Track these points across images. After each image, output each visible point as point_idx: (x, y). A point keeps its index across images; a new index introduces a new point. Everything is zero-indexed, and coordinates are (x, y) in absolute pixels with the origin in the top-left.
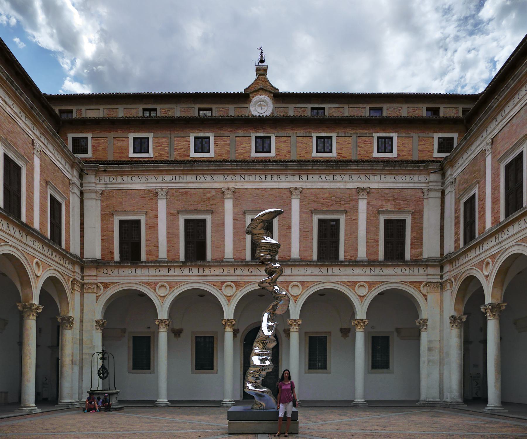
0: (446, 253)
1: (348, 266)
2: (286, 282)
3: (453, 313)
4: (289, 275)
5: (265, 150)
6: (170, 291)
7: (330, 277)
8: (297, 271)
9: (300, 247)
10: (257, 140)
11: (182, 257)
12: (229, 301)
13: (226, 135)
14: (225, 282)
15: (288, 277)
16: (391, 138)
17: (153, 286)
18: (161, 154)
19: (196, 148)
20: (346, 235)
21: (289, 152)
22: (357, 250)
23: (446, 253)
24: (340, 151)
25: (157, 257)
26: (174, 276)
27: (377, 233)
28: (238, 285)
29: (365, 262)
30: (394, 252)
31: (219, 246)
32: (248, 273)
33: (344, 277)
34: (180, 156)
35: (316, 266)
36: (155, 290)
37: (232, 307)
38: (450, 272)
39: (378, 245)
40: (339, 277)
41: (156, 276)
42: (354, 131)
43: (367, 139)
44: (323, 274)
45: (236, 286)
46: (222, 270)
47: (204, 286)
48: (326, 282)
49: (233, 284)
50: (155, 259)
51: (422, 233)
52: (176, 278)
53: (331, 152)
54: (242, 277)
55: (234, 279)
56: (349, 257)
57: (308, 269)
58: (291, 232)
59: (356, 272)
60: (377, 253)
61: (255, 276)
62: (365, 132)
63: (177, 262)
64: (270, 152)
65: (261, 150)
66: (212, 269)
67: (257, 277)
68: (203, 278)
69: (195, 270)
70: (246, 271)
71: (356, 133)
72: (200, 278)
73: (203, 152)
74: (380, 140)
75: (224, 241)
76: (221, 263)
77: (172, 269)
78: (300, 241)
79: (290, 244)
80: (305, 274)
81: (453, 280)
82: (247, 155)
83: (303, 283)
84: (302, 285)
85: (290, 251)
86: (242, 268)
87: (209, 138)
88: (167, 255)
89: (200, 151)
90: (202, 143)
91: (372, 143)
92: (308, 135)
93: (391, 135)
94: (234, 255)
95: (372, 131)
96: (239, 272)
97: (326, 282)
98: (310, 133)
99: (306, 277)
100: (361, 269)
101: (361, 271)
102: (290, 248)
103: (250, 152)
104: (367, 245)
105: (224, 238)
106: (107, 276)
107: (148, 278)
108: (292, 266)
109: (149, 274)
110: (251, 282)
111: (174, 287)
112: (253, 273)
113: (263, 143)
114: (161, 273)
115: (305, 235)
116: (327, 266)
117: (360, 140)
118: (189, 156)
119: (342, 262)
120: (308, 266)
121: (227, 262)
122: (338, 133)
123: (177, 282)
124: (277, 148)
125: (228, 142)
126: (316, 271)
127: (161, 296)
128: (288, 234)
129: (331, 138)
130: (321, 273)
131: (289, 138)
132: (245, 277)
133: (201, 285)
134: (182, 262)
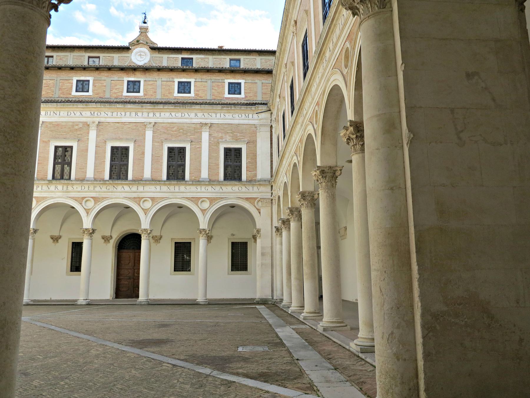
1: (192, 184)
5: (135, 90)
7: (177, 194)
8: (147, 188)
9: (152, 169)
10: (129, 83)
11: (50, 177)
12: (88, 213)
13: (103, 79)
14: (85, 197)
15: (141, 194)
16: (240, 84)
18: (48, 93)
19: (78, 89)
20: (191, 160)
21: (155, 92)
24: (197, 93)
26: (41, 192)
27: (218, 158)
28: (96, 200)
29: (207, 182)
31: (83, 167)
33: (188, 194)
34: (63, 94)
35: (165, 185)
37: (90, 218)
39: (218, 168)
40: (184, 194)
42: (209, 78)
43: (220, 84)
44: (171, 191)
46: (83, 188)
47: (67, 200)
49: (91, 199)
51: (256, 158)
52: (43, 194)
53: (190, 93)
54: (100, 193)
55: (94, 195)
56: (193, 178)
57: (158, 187)
59: (199, 190)
60: (218, 174)
62: (218, 78)
63: (44, 180)
64: (139, 92)
65: (132, 91)
66: (75, 187)
67: (113, 194)
68: (66, 194)
69: (60, 187)
70: (104, 189)
72: (64, 194)
73: (83, 91)
74: (231, 85)
75: (86, 164)
76: (82, 180)
79: (143, 167)
80: (155, 191)
82: (119, 94)
83: (153, 199)
87: (89, 81)
89: (81, 90)
90: (82, 84)
91: (224, 87)
92: (171, 80)
93: (239, 81)
94: (94, 175)
95: (224, 78)
96: (98, 189)
98: (173, 78)
99: (156, 194)
100: (203, 188)
102: (143, 170)
103: (122, 92)
105: (87, 161)
108: (144, 185)
111: (40, 201)
112: (110, 190)
113: (134, 85)
115: (156, 159)
116: (174, 184)
117: (214, 84)
118: (71, 94)
119: (186, 181)
120: (157, 184)
121: (87, 181)
123: (44, 197)
124: (144, 90)
125: (105, 84)
126: (165, 188)
129: (190, 83)
132: (103, 194)
133: (64, 200)
134: (49, 181)
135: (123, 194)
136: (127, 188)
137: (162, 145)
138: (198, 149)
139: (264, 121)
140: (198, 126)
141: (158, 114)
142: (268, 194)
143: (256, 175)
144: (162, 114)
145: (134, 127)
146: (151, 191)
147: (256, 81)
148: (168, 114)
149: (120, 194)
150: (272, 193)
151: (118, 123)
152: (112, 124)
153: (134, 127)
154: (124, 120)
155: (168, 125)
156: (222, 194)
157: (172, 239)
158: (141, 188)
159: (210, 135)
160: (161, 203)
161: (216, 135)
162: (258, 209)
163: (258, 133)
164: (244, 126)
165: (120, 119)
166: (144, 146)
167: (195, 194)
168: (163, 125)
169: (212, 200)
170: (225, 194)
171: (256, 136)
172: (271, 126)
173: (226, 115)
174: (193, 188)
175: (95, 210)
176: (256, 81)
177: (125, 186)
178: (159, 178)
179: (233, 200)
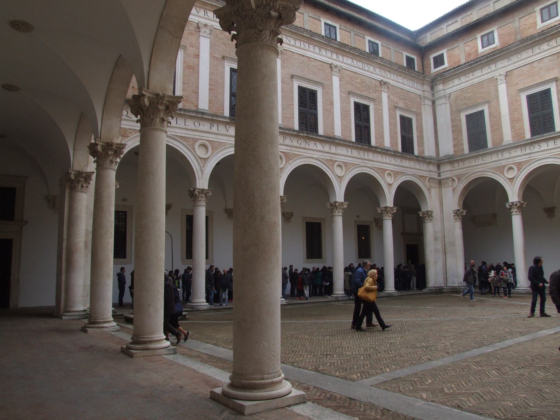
0: (442, 155)
2: (332, 160)
3: (456, 207)
4: (334, 154)
6: (212, 153)
17: (191, 143)
22: (383, 137)
23: (442, 155)
25: (197, 106)
26: (218, 134)
30: (407, 146)
32: (297, 145)
33: (376, 163)
35: (356, 148)
36: (194, 149)
38: (451, 171)
41: (196, 131)
42: (351, 28)
45: (285, 157)
48: (364, 166)
50: (193, 108)
52: (220, 137)
56: (378, 144)
58: (333, 108)
60: (397, 144)
61: (305, 149)
67: (305, 151)
71: (354, 31)
77: (215, 125)
78: (341, 120)
81: (454, 178)
84: (345, 166)
85: (333, 128)
86: (292, 138)
88: (209, 106)
91: (364, 43)
92: (317, 18)
93: (377, 42)
97: (364, 166)
99: (347, 158)
101: (387, 159)
104: (390, 136)
106: (128, 120)
107: (184, 131)
109: (187, 127)
110: (301, 155)
111: (217, 149)
112: (302, 146)
114: (202, 128)
122: (340, 26)
126: (355, 153)
127: (201, 158)
128: (331, 109)
130: (359, 156)
131: (302, 15)
132: (294, 149)
135: (316, 153)
136: (319, 146)
137: (349, 97)
138: (380, 111)
139: (428, 93)
140: (378, 84)
141: (340, 58)
142: (435, 174)
143: (423, 152)
144: (345, 58)
145: (320, 67)
146: (344, 154)
147: (390, 47)
148: (349, 61)
149: (311, 154)
150: (439, 174)
151: (303, 56)
152: (297, 56)
153: (320, 67)
154: (309, 54)
155: (352, 74)
156: (403, 168)
157: (303, 218)
158: (333, 149)
159: (388, 97)
160: (353, 171)
161: (392, 97)
162: (429, 190)
163: (422, 106)
164: (413, 95)
165: (305, 52)
166: (332, 95)
167: (381, 164)
168: (347, 72)
169: (396, 174)
170: (405, 169)
171: (421, 108)
172: (434, 103)
173: (398, 77)
174: (379, 158)
175: (287, 170)
176: (390, 47)
177: (317, 143)
178: (348, 139)
179: (410, 177)
